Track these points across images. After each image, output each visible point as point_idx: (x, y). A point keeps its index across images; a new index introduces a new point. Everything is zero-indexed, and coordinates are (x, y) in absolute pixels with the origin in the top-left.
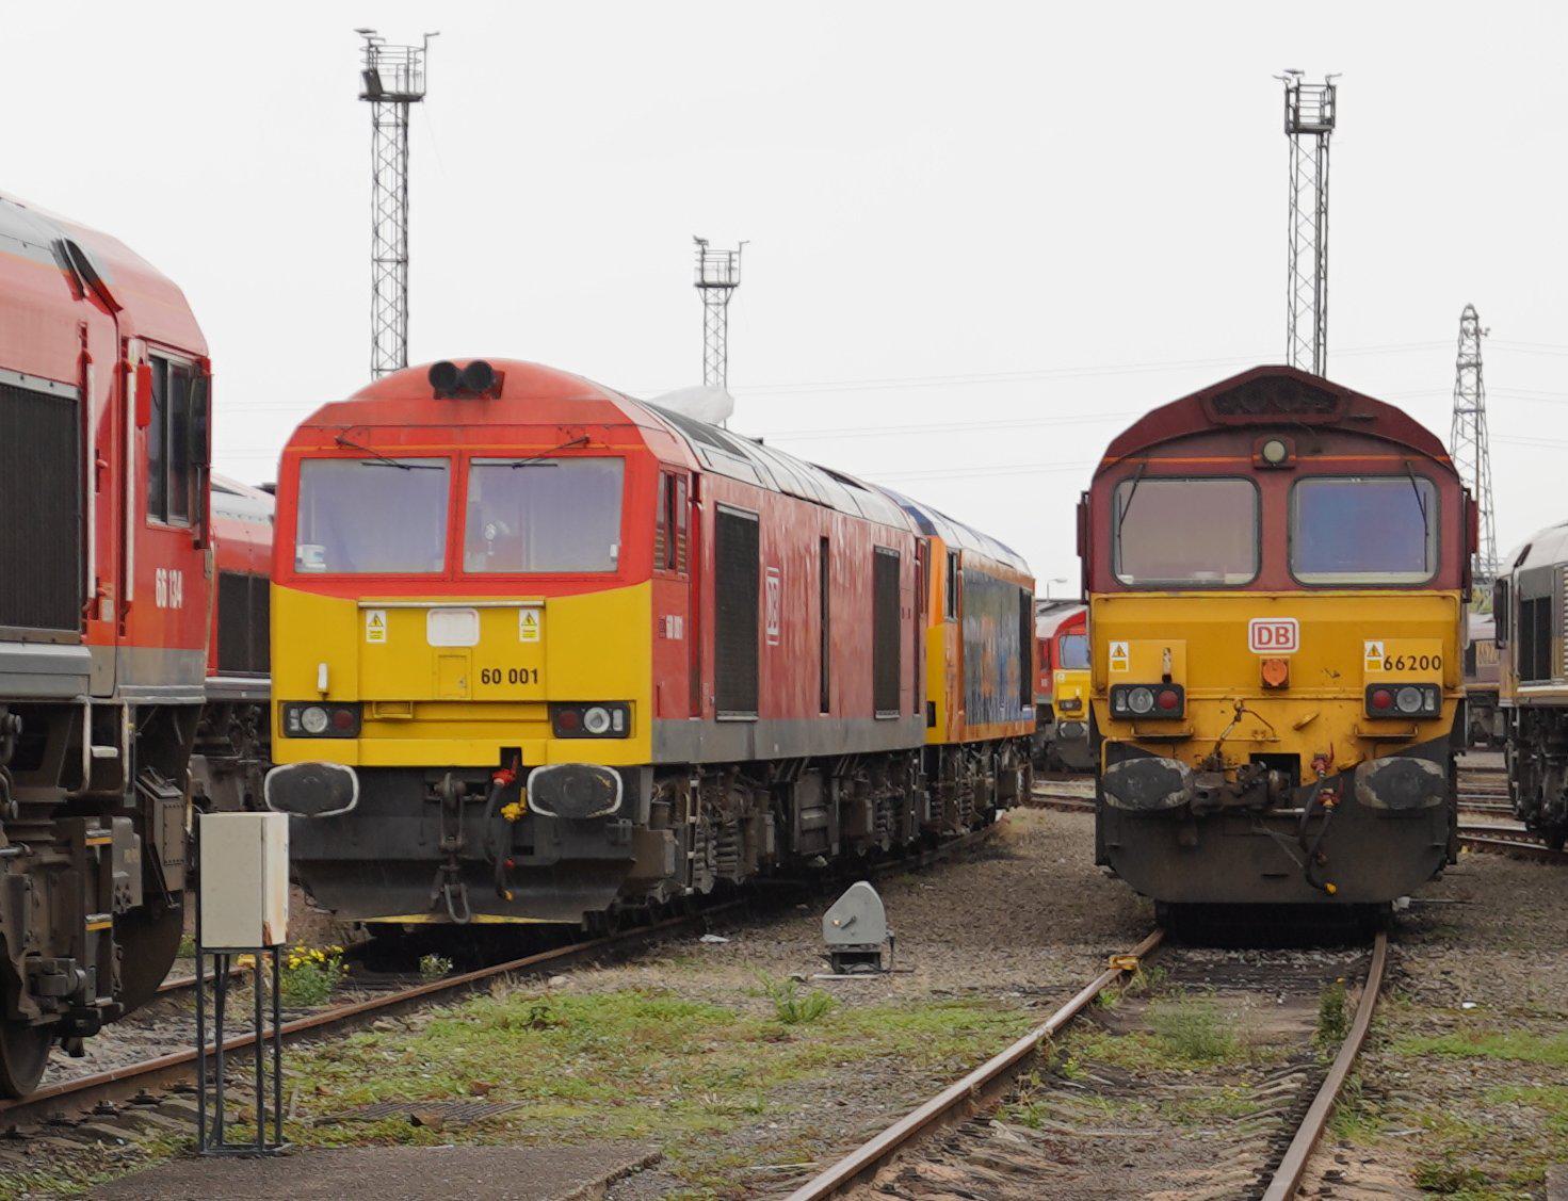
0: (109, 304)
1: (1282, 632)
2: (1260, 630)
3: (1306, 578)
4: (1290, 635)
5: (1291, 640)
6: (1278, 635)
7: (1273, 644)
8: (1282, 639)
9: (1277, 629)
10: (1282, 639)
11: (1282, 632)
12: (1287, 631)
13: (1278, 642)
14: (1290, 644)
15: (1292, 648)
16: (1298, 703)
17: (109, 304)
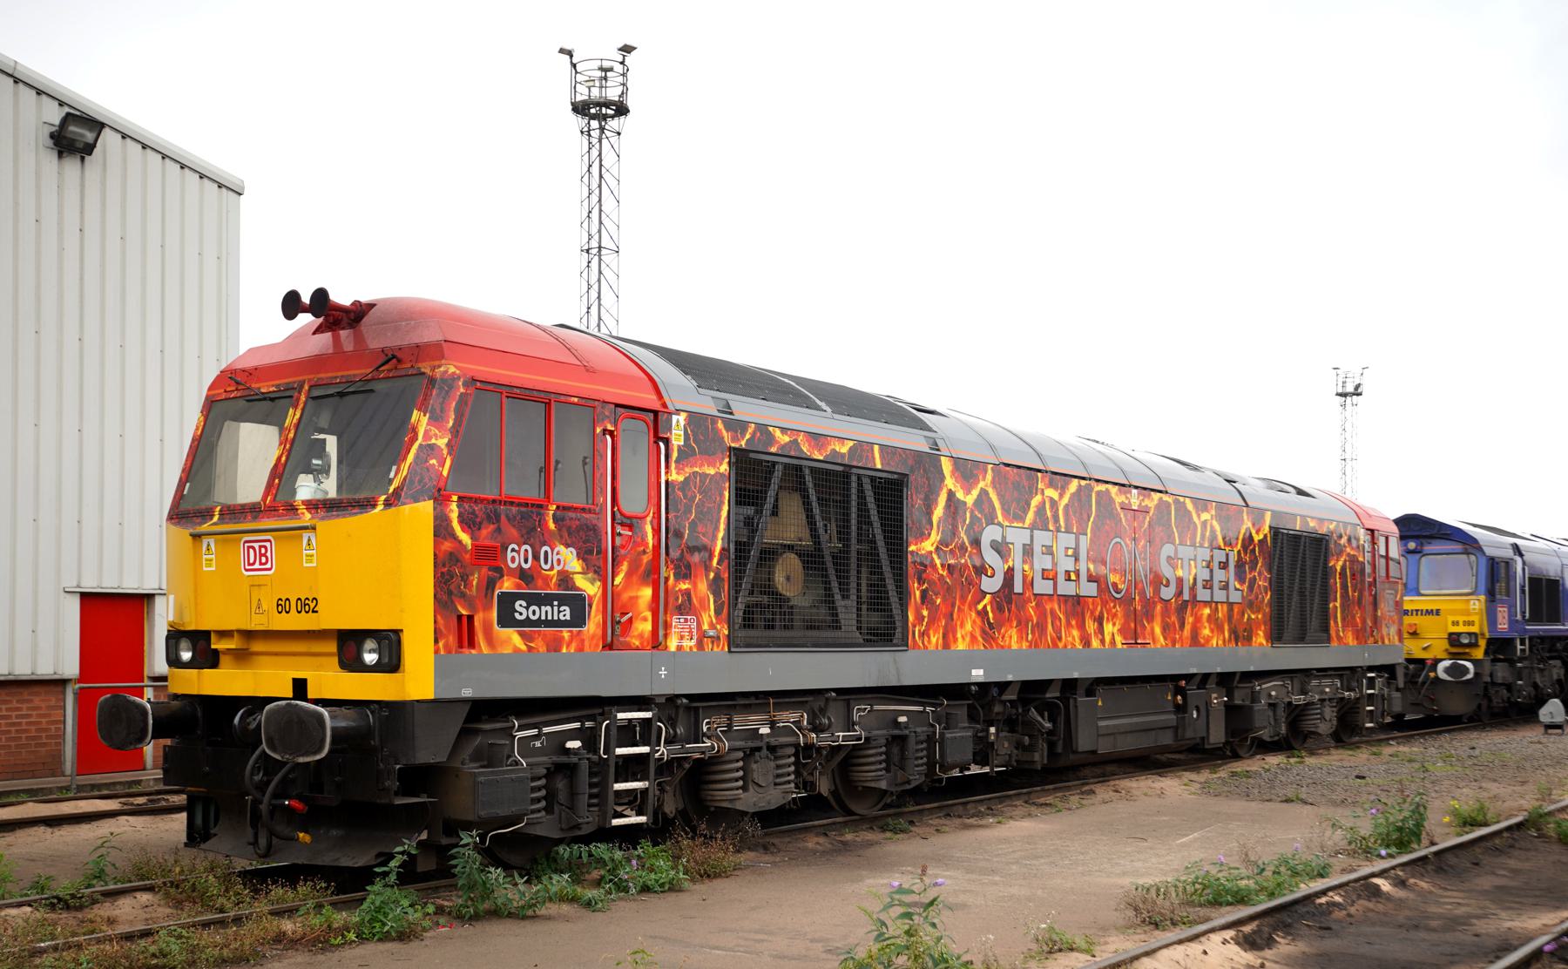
0: (1521, 555)
1: (263, 551)
2: (249, 547)
3: (1422, 592)
4: (269, 554)
5: (270, 559)
6: (261, 555)
7: (257, 566)
8: (264, 560)
9: (260, 547)
11: (263, 551)
12: (266, 547)
13: (261, 564)
14: (268, 566)
15: (270, 569)
17: (1521, 555)
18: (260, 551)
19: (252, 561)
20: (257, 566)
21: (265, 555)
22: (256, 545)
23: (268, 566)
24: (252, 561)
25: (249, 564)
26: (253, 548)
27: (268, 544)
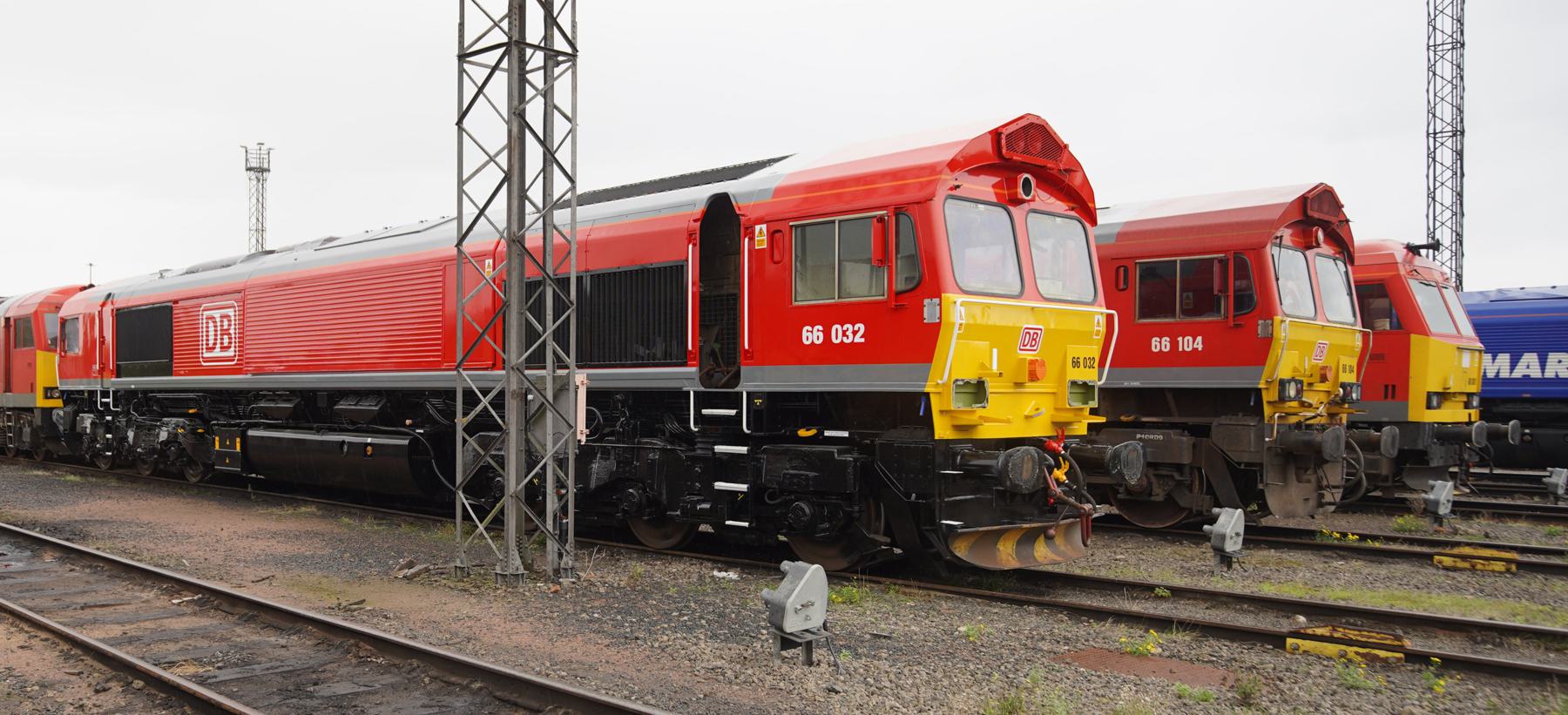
6: (1034, 339)
8: (1034, 342)
9: (1034, 333)
10: (1034, 342)
12: (1037, 334)
13: (1031, 346)
14: (1035, 348)
15: (1035, 350)
16: (1025, 396)
18: (222, 326)
19: (1026, 343)
20: (1028, 347)
21: (1035, 340)
22: (1032, 332)
23: (1035, 348)
24: (1026, 343)
25: (1024, 346)
26: (1029, 333)
27: (1039, 332)
